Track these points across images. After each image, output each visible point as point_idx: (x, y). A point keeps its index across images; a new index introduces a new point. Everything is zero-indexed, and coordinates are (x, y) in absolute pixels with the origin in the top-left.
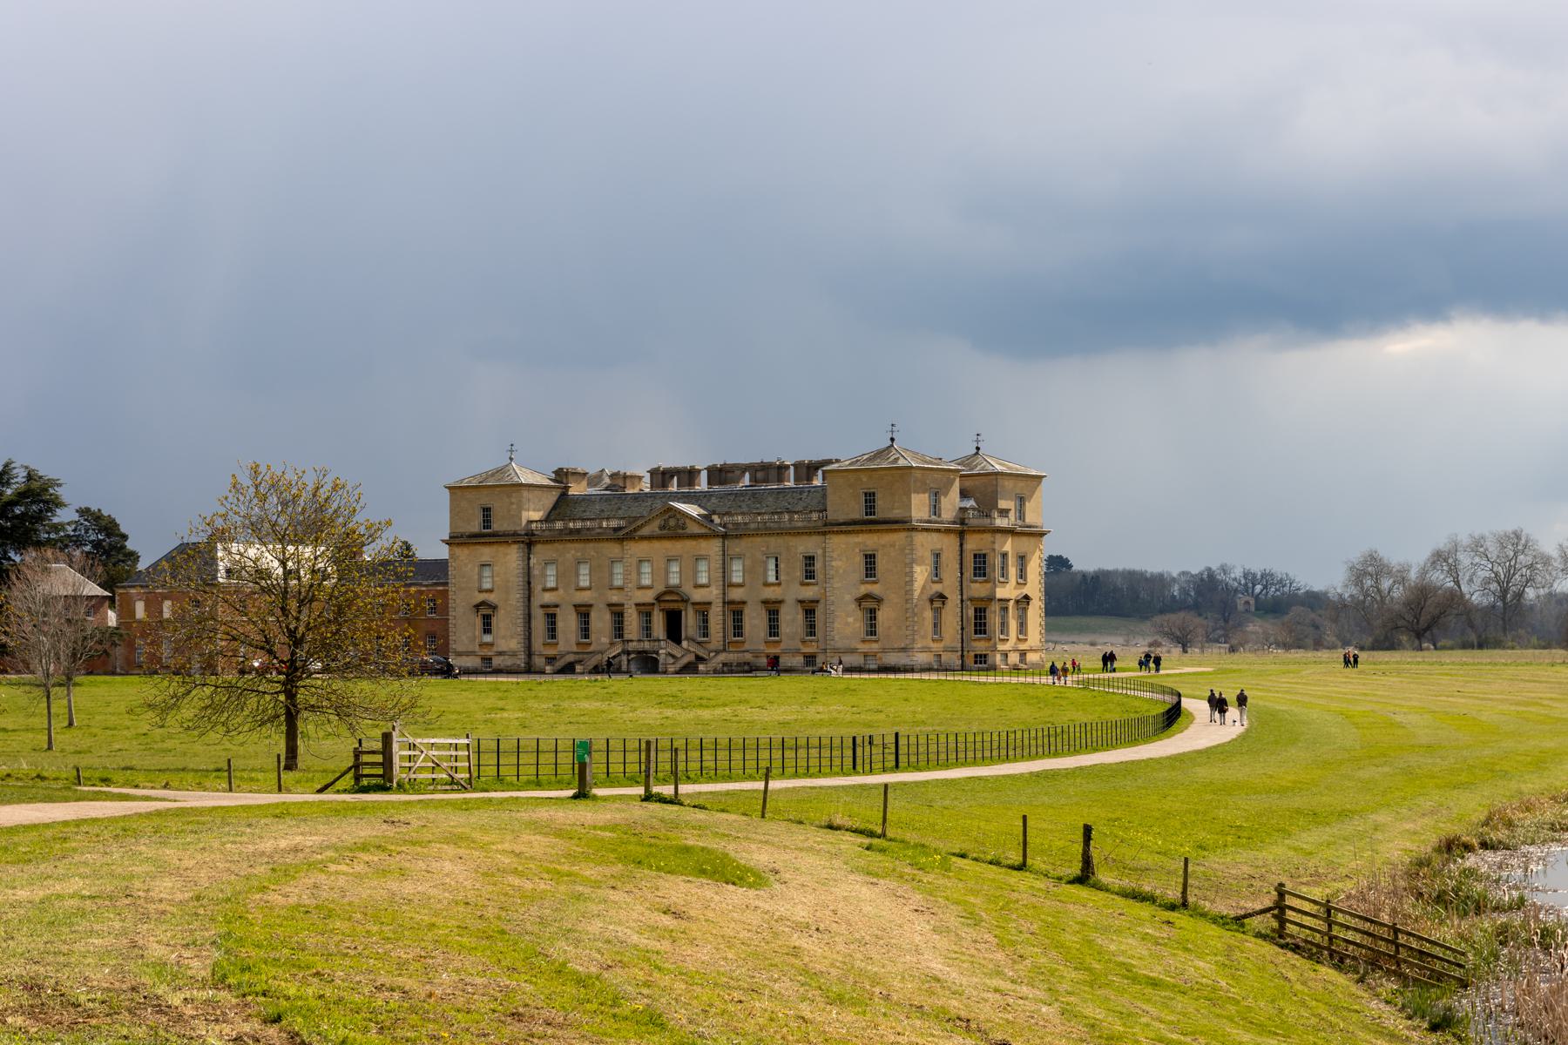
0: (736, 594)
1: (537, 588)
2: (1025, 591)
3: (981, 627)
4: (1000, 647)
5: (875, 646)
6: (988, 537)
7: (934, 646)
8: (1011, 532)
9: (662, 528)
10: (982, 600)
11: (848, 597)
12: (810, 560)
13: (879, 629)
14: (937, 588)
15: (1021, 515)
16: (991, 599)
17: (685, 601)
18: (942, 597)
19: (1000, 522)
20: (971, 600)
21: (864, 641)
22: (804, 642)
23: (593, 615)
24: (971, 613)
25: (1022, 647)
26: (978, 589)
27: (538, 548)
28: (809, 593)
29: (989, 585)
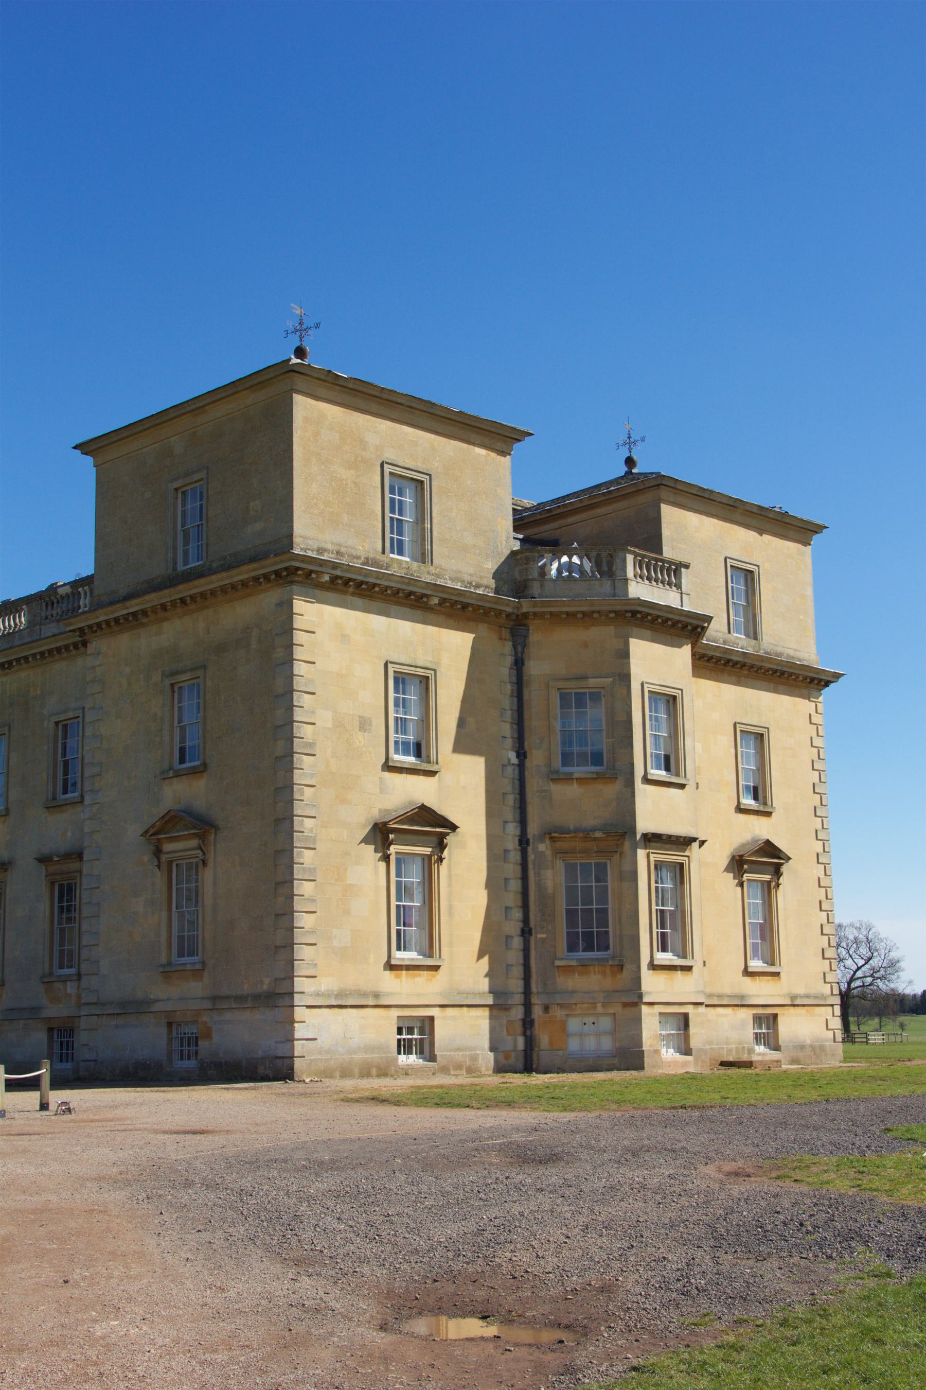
2: (760, 829)
4: (653, 985)
5: (196, 989)
6: (601, 634)
8: (683, 628)
10: (586, 834)
11: (133, 832)
15: (753, 632)
16: (620, 832)
18: (431, 826)
19: (640, 590)
21: (168, 972)
22: (48, 981)
24: (552, 878)
25: (762, 992)
26: (573, 802)
28: (57, 830)
29: (610, 790)
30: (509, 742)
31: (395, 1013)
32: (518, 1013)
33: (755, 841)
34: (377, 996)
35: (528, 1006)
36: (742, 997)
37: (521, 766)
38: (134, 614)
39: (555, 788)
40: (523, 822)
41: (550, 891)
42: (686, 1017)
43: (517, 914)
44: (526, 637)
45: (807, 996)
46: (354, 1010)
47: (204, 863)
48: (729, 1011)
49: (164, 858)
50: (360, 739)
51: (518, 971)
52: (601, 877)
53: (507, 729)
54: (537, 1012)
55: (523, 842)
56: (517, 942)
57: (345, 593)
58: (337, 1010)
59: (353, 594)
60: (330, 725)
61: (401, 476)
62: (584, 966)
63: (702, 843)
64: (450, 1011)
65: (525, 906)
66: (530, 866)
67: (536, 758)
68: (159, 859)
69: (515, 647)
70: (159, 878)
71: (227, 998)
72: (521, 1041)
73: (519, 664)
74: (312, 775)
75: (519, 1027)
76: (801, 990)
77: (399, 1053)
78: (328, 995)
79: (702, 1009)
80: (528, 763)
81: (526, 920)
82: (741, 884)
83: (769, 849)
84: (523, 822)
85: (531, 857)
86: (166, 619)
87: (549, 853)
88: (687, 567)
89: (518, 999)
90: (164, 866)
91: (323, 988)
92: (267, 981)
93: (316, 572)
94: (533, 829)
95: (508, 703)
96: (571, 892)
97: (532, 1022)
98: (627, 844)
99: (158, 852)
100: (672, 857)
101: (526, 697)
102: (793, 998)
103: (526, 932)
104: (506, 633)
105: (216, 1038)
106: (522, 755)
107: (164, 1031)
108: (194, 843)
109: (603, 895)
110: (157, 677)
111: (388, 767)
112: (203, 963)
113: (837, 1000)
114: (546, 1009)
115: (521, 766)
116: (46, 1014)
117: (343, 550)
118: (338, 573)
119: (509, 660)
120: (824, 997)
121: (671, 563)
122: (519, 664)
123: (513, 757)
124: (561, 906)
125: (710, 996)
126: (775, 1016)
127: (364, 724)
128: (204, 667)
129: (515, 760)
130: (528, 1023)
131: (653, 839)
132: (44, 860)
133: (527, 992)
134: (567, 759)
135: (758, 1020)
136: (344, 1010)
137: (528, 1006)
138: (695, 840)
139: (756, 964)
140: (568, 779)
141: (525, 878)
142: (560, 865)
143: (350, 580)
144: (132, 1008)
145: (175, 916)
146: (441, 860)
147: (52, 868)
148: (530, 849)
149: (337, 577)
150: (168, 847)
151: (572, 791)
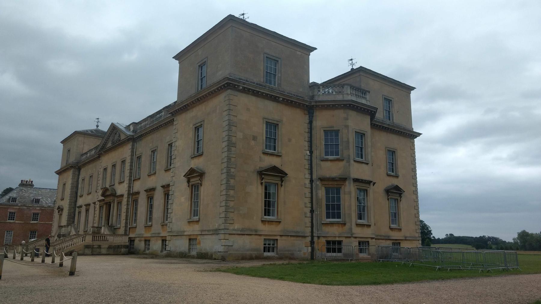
0: (137, 186)
1: (79, 194)
2: (395, 182)
3: (334, 210)
7: (266, 229)
9: (113, 143)
10: (333, 179)
12: (170, 145)
13: (201, 208)
14: (270, 161)
17: (114, 195)
18: (278, 173)
20: (322, 179)
23: (90, 211)
24: (321, 193)
25: (395, 235)
27: (83, 170)
29: (341, 164)
30: (307, 148)
31: (263, 237)
32: (309, 239)
33: (392, 185)
34: (256, 231)
35: (312, 237)
36: (389, 237)
37: (311, 156)
38: (185, 106)
39: (323, 163)
40: (311, 174)
41: (320, 197)
42: (368, 242)
43: (309, 205)
44: (313, 113)
45: (410, 237)
46: (248, 236)
47: (201, 185)
48: (384, 241)
49: (191, 184)
50: (253, 143)
51: (309, 224)
52: (338, 193)
53: (307, 144)
54: (315, 239)
55: (312, 181)
56: (309, 214)
57: (248, 94)
58: (241, 236)
59: (252, 95)
60: (242, 137)
61: (270, 58)
62: (332, 224)
63: (374, 184)
64: (284, 238)
65: (312, 202)
66: (314, 189)
67: (316, 153)
68: (189, 184)
69: (309, 117)
70: (188, 191)
71: (205, 231)
72: (310, 248)
73: (311, 123)
74: (234, 154)
75: (309, 244)
76: (408, 235)
77: (264, 251)
78: (238, 230)
79: (374, 240)
80: (314, 155)
81: (312, 207)
82: (388, 199)
83: (397, 188)
84: (311, 174)
85: (314, 186)
86: (195, 107)
87: (320, 185)
88: (369, 92)
89: (309, 234)
90: (190, 186)
91: (236, 227)
92: (217, 225)
93: (237, 85)
94: (314, 177)
95: (307, 135)
96: (328, 199)
97: (314, 242)
98: (347, 183)
99: (188, 182)
100: (363, 186)
101: (313, 133)
102: (406, 237)
103: (312, 211)
104: (306, 112)
105: (202, 245)
106: (311, 152)
107: (188, 241)
108: (198, 179)
109: (339, 199)
110: (191, 126)
111: (264, 153)
112: (199, 219)
113: (420, 239)
114: (319, 237)
115: (311, 156)
116: (162, 235)
117: (248, 80)
118: (245, 86)
119: (307, 121)
120: (415, 237)
121: (364, 90)
122: (311, 123)
123: (308, 153)
124: (324, 203)
125: (377, 236)
126: (400, 243)
127: (255, 138)
128: (204, 121)
129: (309, 154)
130: (312, 242)
131: (356, 180)
132: (163, 187)
133: (312, 232)
134: (327, 154)
135: (394, 244)
136: (243, 236)
137: (312, 237)
138: (371, 182)
139: (393, 226)
140: (327, 160)
141: (312, 193)
142: (323, 189)
143: (250, 89)
144: (180, 235)
145: (193, 203)
146: (282, 185)
147: (165, 190)
148: (313, 183)
149: (245, 88)
150: (191, 180)
151: (328, 164)
